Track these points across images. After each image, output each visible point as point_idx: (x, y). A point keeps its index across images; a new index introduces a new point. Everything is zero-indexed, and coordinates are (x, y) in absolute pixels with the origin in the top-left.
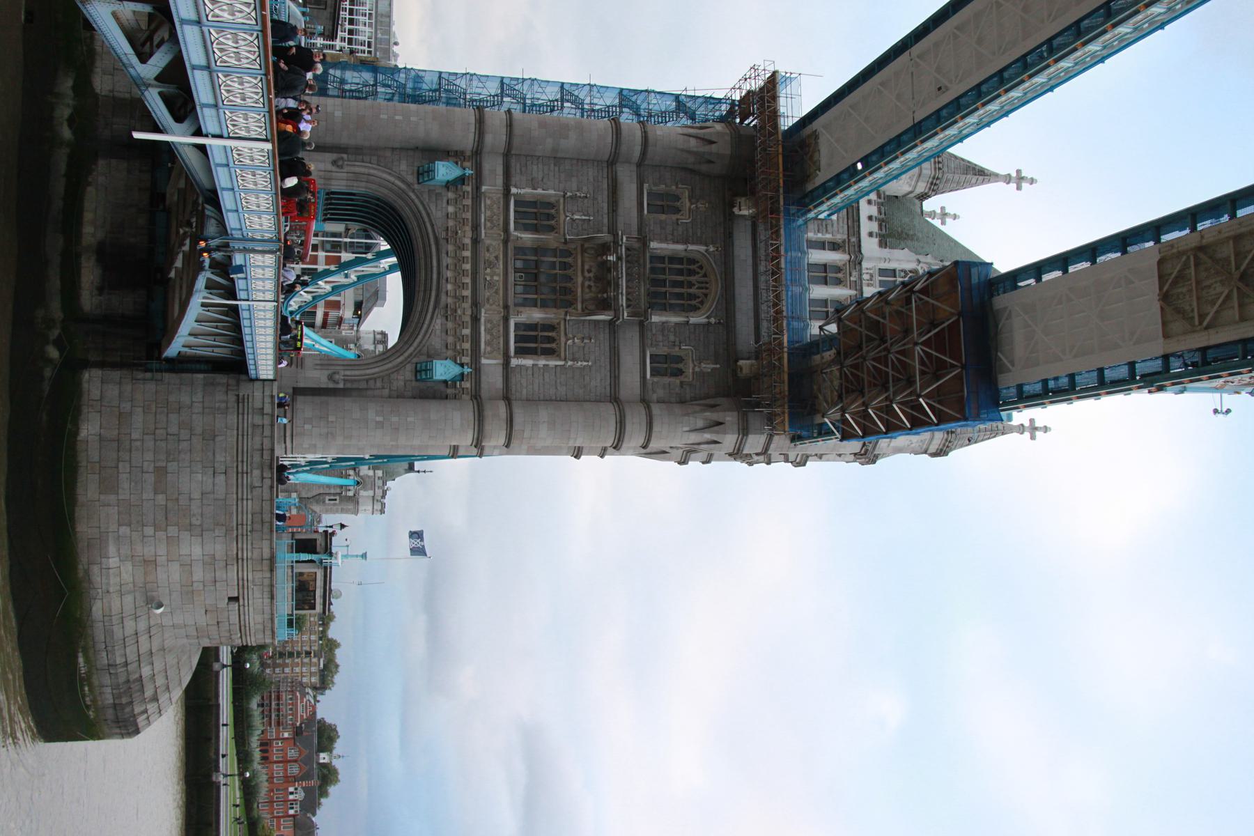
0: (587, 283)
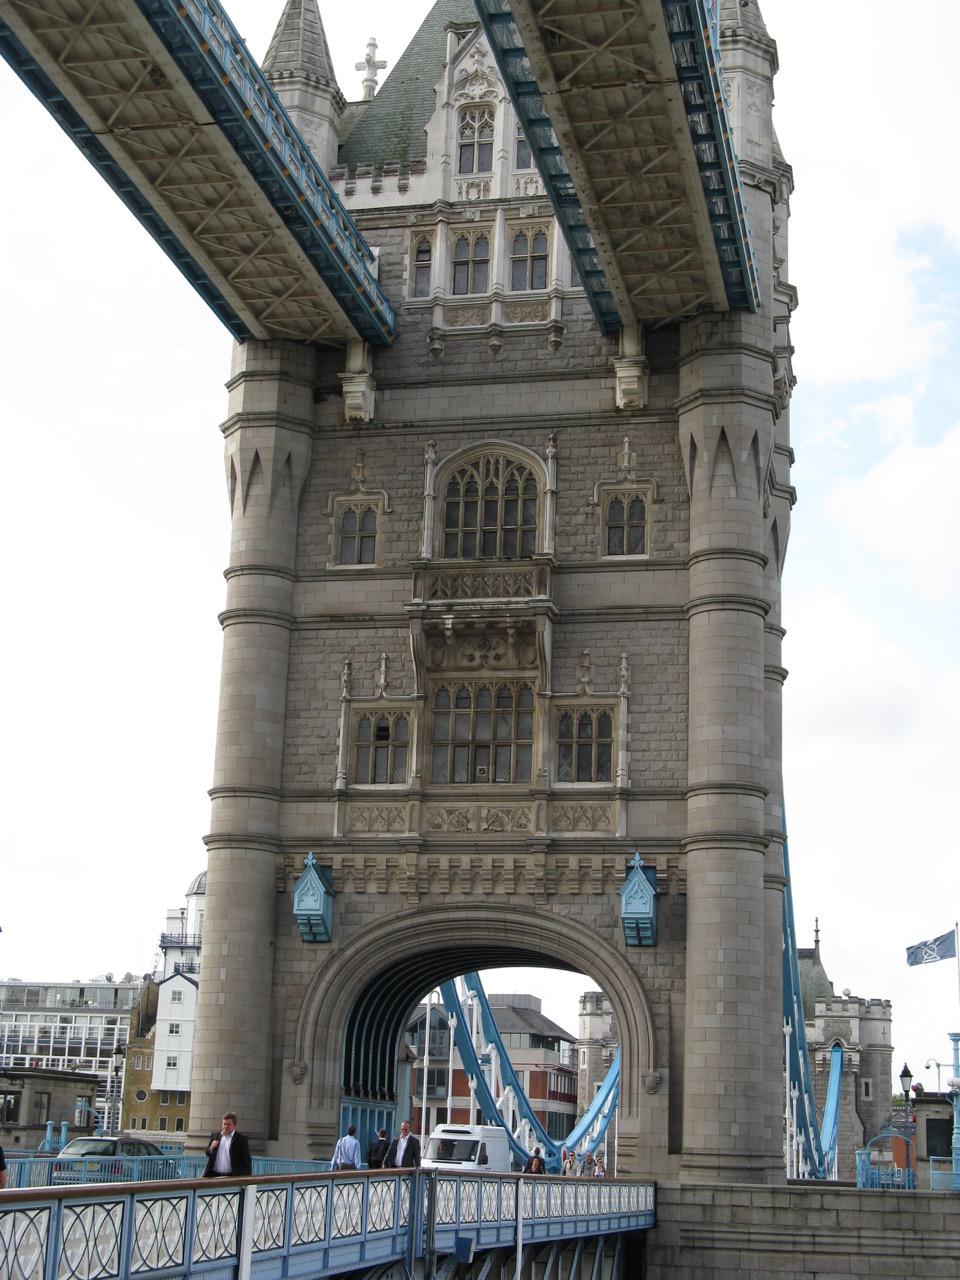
0: (492, 662)
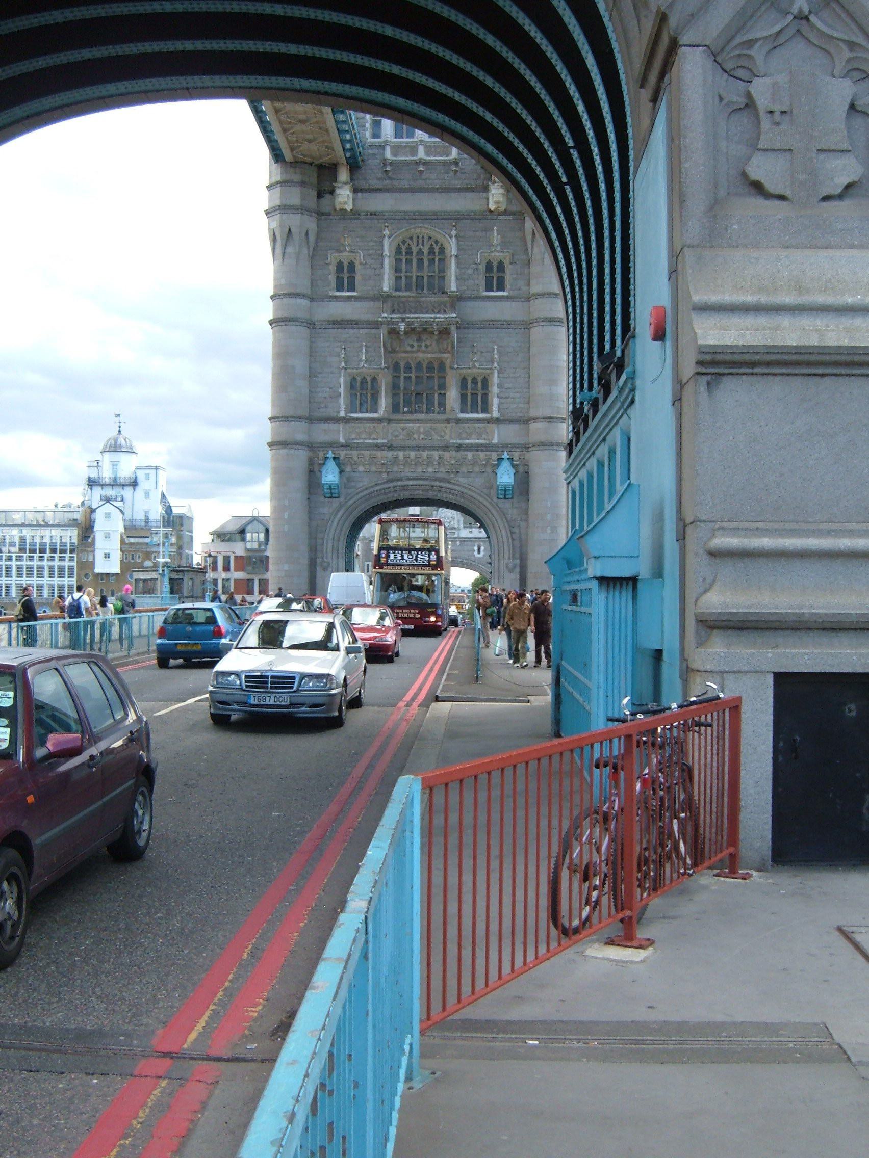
0: (423, 348)
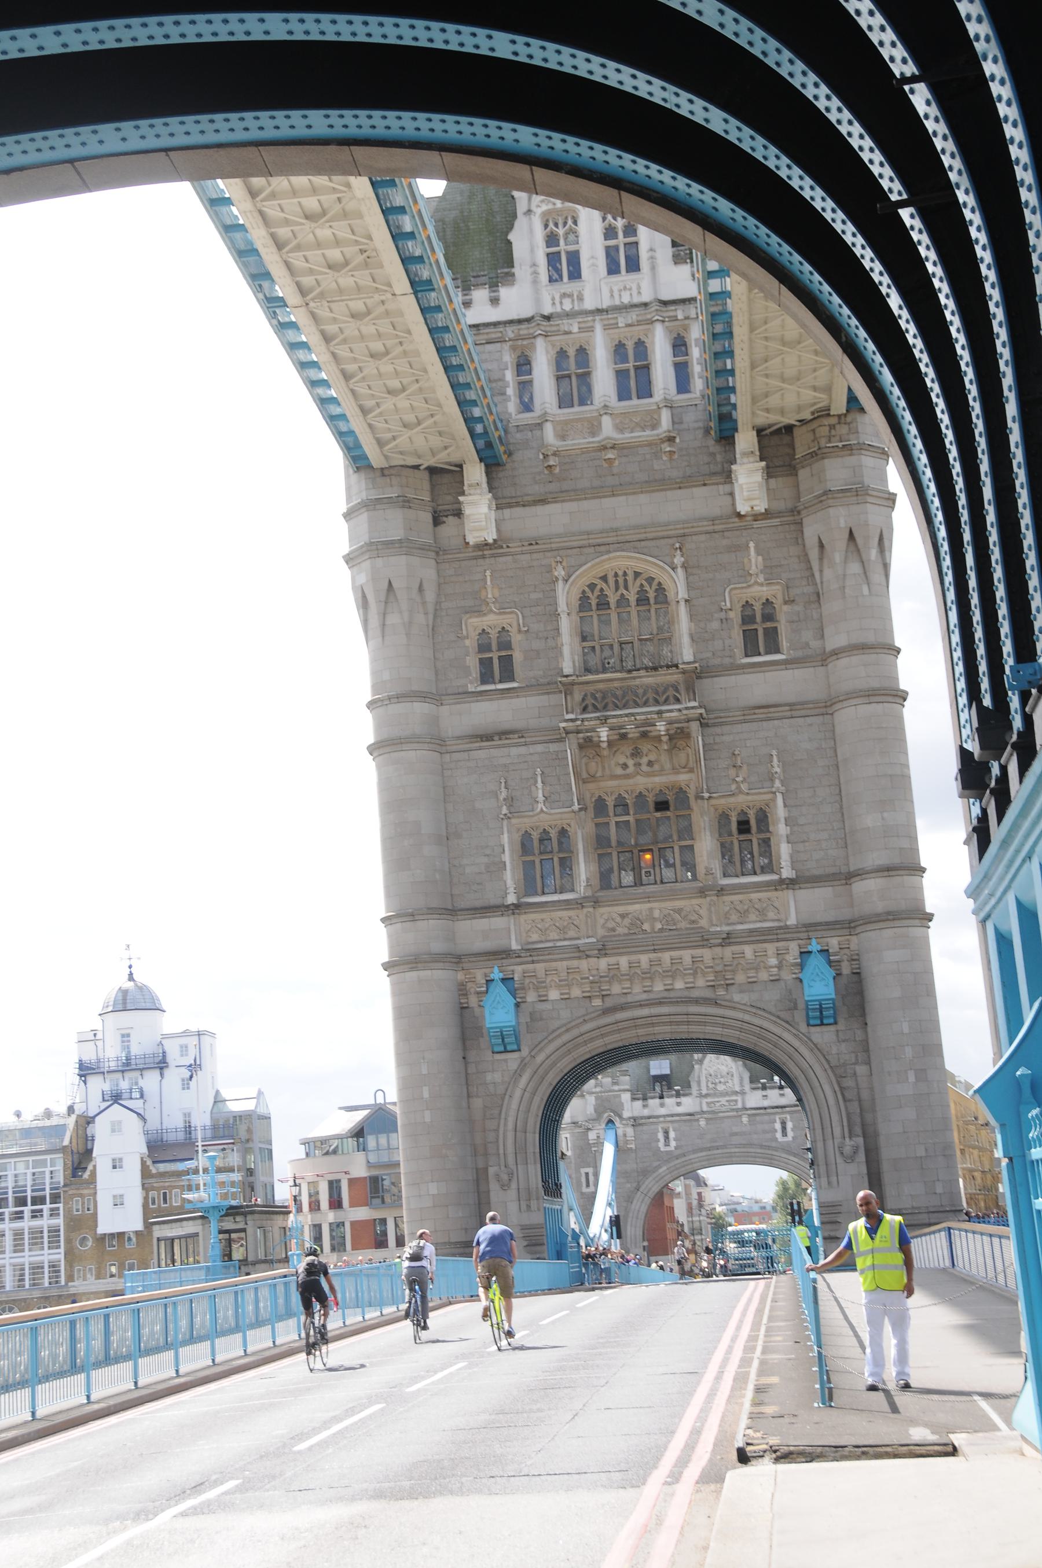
0: (645, 768)
